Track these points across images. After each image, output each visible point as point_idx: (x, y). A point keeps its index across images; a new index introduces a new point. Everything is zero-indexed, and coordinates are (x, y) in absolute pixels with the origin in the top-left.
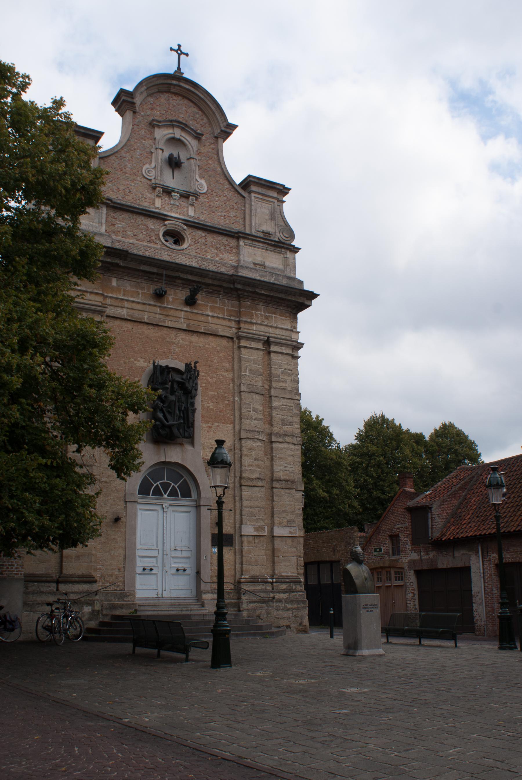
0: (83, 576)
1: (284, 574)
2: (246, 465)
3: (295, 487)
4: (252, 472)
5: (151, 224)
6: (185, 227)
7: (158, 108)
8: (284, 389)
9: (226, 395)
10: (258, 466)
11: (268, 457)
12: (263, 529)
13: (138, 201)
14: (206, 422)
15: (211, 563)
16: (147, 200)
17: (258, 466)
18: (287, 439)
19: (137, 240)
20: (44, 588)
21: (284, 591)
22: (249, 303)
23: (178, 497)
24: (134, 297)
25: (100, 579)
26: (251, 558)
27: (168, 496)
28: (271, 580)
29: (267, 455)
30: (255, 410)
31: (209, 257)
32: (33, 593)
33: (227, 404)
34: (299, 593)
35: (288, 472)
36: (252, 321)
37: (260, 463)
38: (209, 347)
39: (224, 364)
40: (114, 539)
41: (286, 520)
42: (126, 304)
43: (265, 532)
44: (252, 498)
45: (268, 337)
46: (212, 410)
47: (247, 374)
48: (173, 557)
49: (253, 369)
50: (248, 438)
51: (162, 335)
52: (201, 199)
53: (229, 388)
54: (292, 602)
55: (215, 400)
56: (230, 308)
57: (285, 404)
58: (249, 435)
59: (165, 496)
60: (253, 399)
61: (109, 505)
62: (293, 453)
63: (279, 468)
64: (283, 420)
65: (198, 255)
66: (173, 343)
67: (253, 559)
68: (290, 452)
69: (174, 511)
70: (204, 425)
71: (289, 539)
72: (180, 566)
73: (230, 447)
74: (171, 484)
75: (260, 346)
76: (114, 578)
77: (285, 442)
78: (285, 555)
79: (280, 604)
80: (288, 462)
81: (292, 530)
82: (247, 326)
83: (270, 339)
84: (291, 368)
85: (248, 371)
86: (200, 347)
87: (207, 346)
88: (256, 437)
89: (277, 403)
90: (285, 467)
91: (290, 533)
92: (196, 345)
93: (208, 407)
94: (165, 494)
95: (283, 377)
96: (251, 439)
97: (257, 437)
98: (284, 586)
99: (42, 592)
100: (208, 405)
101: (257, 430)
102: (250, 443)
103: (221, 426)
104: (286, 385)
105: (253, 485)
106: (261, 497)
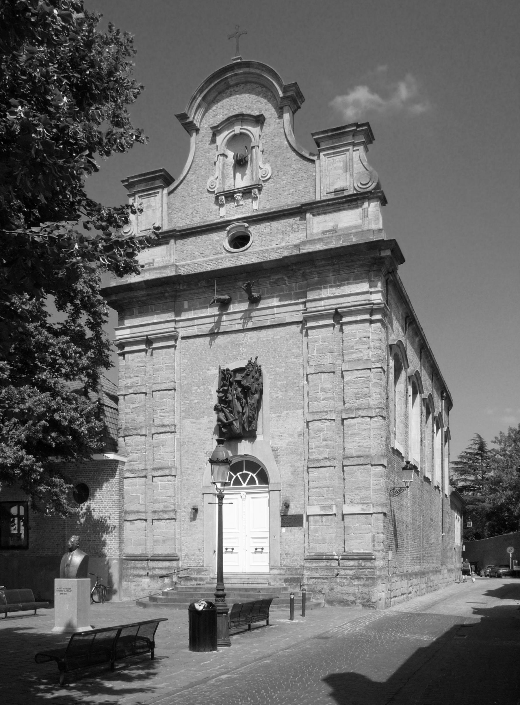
0: (168, 555)
1: (355, 551)
2: (314, 446)
3: (369, 462)
4: (320, 453)
5: (215, 236)
6: (246, 225)
7: (221, 111)
8: (359, 360)
9: (295, 381)
10: (327, 446)
11: (340, 435)
12: (330, 507)
13: (205, 218)
14: (275, 413)
15: (280, 542)
16: (213, 213)
17: (327, 446)
18: (361, 413)
19: (204, 257)
20: (139, 564)
21: (351, 568)
22: (316, 279)
23: (255, 484)
24: (203, 313)
25: (185, 557)
26: (318, 536)
27: (247, 484)
28: (337, 557)
29: (339, 434)
30: (323, 390)
31: (274, 246)
32: (131, 568)
33: (297, 390)
34: (369, 570)
35: (362, 447)
36: (321, 297)
37: (329, 443)
38: (277, 337)
39: (294, 351)
40: (195, 525)
41: (359, 497)
42: (196, 322)
43: (332, 511)
44: (319, 478)
45: (336, 309)
46: (281, 399)
47: (315, 354)
48: (253, 538)
49: (321, 347)
50: (315, 420)
51: (231, 340)
52: (266, 186)
53: (299, 374)
54: (359, 578)
55: (284, 389)
56: (298, 291)
57: (360, 376)
58: (316, 417)
59: (244, 485)
60: (321, 379)
61: (190, 498)
62: (369, 427)
63: (351, 445)
64: (356, 394)
65: (263, 248)
66: (242, 344)
67: (321, 538)
68: (365, 427)
69: (252, 498)
70: (273, 415)
71: (362, 516)
72: (259, 546)
73: (300, 432)
74: (249, 474)
75: (331, 321)
76: (195, 556)
77: (359, 417)
78: (356, 532)
79: (345, 581)
80: (362, 437)
81: (364, 507)
82: (313, 304)
83: (338, 310)
84: (367, 335)
85: (315, 351)
86: (268, 340)
87: (275, 337)
88: (324, 417)
89: (350, 377)
90: (359, 443)
91: (363, 509)
92: (264, 339)
93: (277, 397)
94: (244, 482)
95: (358, 348)
96: (318, 420)
97: (326, 417)
98: (351, 563)
99: (137, 568)
100: (277, 395)
101: (326, 410)
102: (318, 424)
103: (290, 414)
104: (362, 355)
105: (319, 466)
106: (329, 477)
